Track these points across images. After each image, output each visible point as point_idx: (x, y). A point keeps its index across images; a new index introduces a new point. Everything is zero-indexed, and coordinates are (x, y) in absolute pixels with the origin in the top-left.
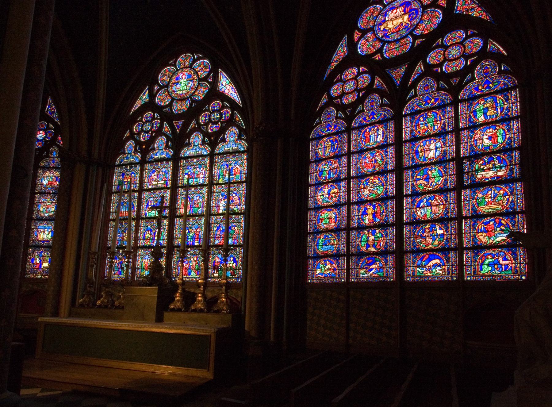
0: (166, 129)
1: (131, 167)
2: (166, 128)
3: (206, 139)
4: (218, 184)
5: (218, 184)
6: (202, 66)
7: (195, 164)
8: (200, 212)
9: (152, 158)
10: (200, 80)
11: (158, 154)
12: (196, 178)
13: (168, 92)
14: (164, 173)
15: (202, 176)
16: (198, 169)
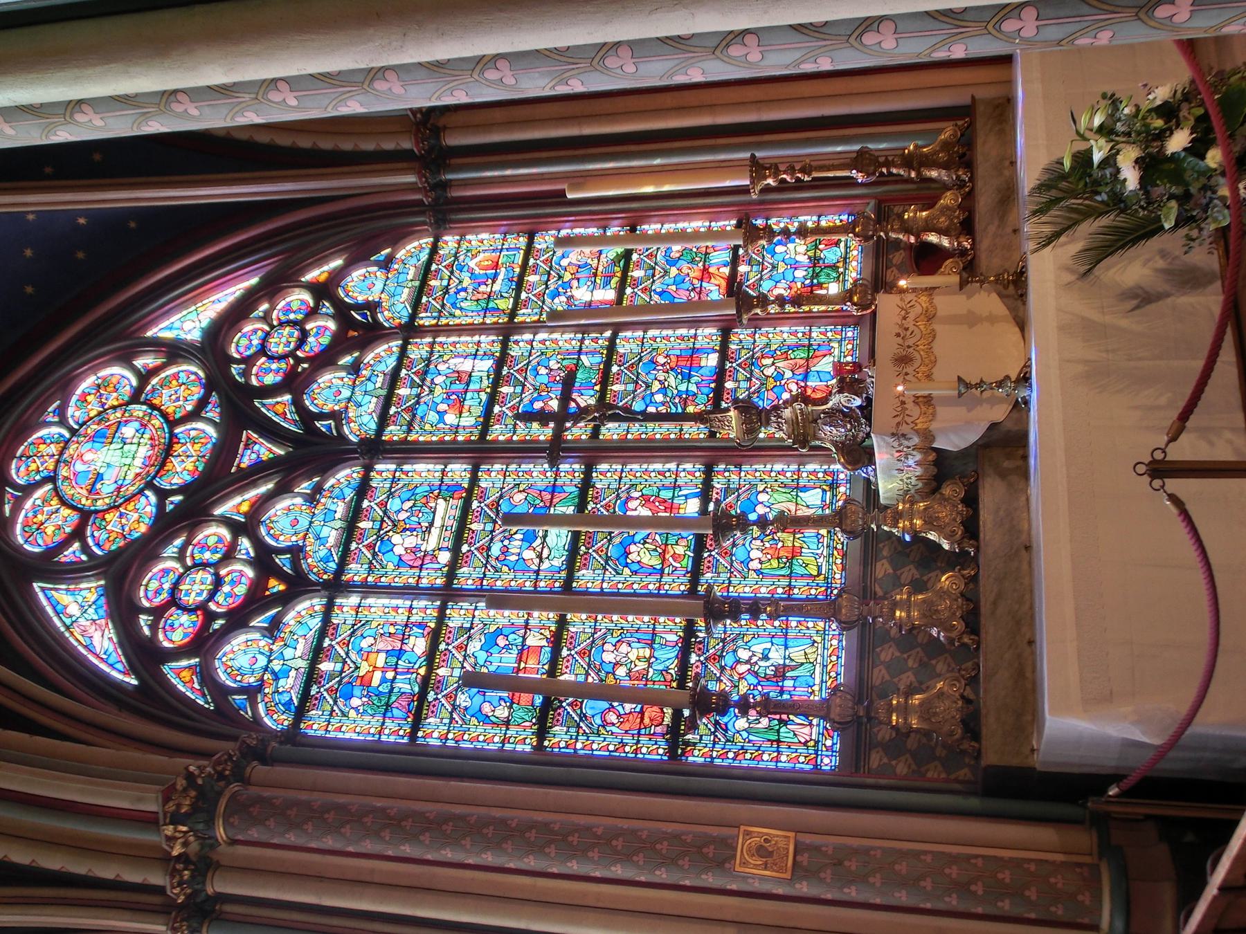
0: (245, 508)
1: (329, 654)
2: (235, 505)
3: (346, 360)
4: (513, 313)
5: (513, 313)
6: (89, 398)
7: (415, 391)
8: (597, 359)
9: (326, 560)
10: (135, 398)
11: (325, 532)
12: (468, 385)
13: (113, 507)
14: (410, 504)
15: (466, 365)
16: (439, 380)
